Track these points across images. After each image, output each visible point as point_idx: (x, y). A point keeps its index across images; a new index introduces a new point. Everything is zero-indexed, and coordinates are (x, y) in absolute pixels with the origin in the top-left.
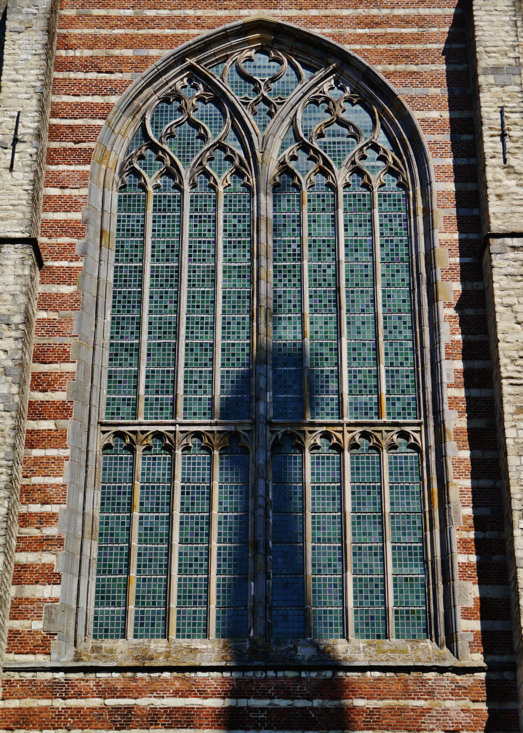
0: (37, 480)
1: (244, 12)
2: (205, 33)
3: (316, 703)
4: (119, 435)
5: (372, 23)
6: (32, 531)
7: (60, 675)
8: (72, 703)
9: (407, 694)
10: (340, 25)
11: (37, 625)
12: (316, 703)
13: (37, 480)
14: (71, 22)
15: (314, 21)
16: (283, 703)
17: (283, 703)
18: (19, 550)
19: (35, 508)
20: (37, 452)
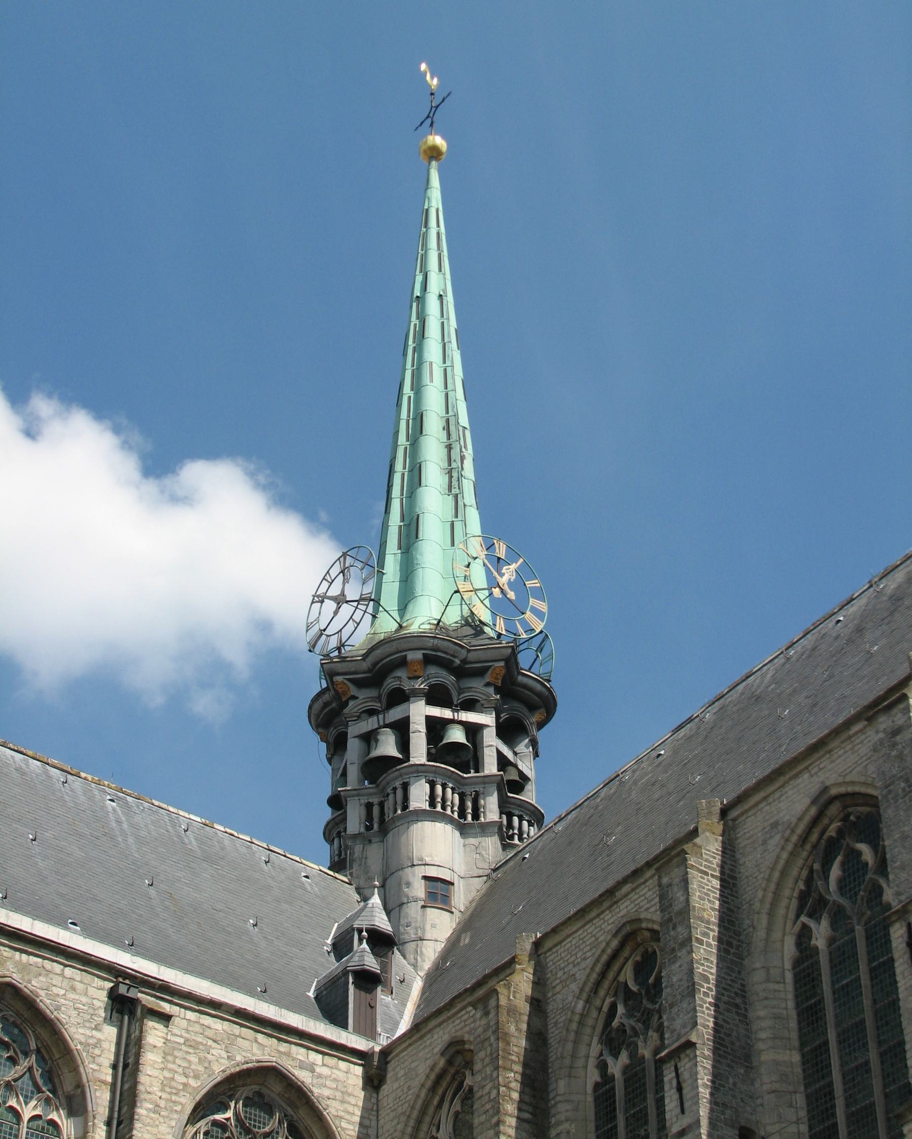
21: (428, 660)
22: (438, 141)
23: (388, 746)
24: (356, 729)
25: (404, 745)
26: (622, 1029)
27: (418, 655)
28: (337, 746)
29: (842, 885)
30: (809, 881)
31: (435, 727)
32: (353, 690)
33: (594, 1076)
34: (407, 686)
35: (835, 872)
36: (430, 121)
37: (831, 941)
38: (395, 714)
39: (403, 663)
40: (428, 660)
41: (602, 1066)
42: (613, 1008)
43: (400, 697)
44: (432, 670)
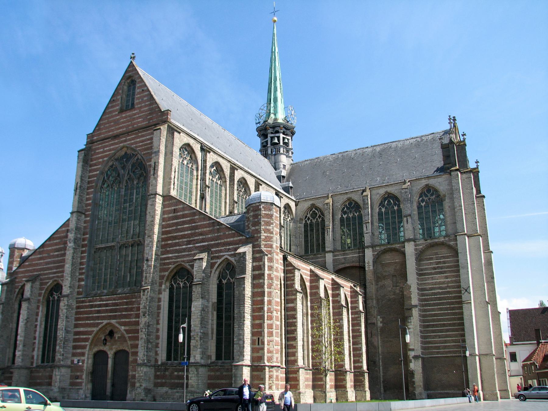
0: (82, 261)
1: (121, 145)
2: (114, 151)
3: (119, 301)
4: (97, 249)
5: (142, 141)
6: (81, 271)
7: (84, 299)
8: (85, 304)
9: (132, 298)
10: (137, 144)
11: (81, 290)
12: (119, 301)
13: (82, 261)
14: (92, 155)
15: (132, 144)
16: (114, 302)
17: (114, 302)
18: (79, 275)
19: (82, 266)
20: (82, 255)
21: (283, 127)
22: (275, 19)
23: (276, 141)
24: (270, 135)
25: (279, 140)
26: (346, 211)
27: (282, 126)
28: (265, 136)
29: (387, 204)
30: (382, 202)
31: (284, 138)
32: (269, 128)
33: (340, 216)
34: (280, 131)
35: (386, 202)
36: (274, 13)
37: (385, 211)
38: (277, 135)
39: (280, 126)
40: (283, 127)
41: (342, 216)
42: (344, 208)
43: (278, 132)
44: (283, 129)
